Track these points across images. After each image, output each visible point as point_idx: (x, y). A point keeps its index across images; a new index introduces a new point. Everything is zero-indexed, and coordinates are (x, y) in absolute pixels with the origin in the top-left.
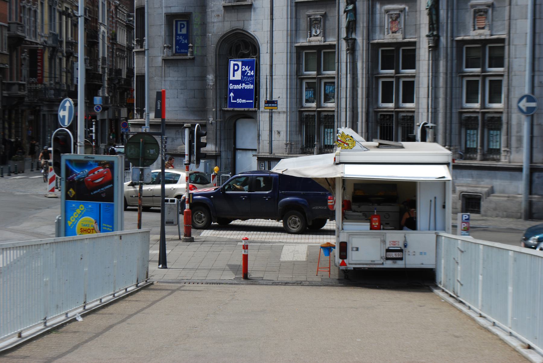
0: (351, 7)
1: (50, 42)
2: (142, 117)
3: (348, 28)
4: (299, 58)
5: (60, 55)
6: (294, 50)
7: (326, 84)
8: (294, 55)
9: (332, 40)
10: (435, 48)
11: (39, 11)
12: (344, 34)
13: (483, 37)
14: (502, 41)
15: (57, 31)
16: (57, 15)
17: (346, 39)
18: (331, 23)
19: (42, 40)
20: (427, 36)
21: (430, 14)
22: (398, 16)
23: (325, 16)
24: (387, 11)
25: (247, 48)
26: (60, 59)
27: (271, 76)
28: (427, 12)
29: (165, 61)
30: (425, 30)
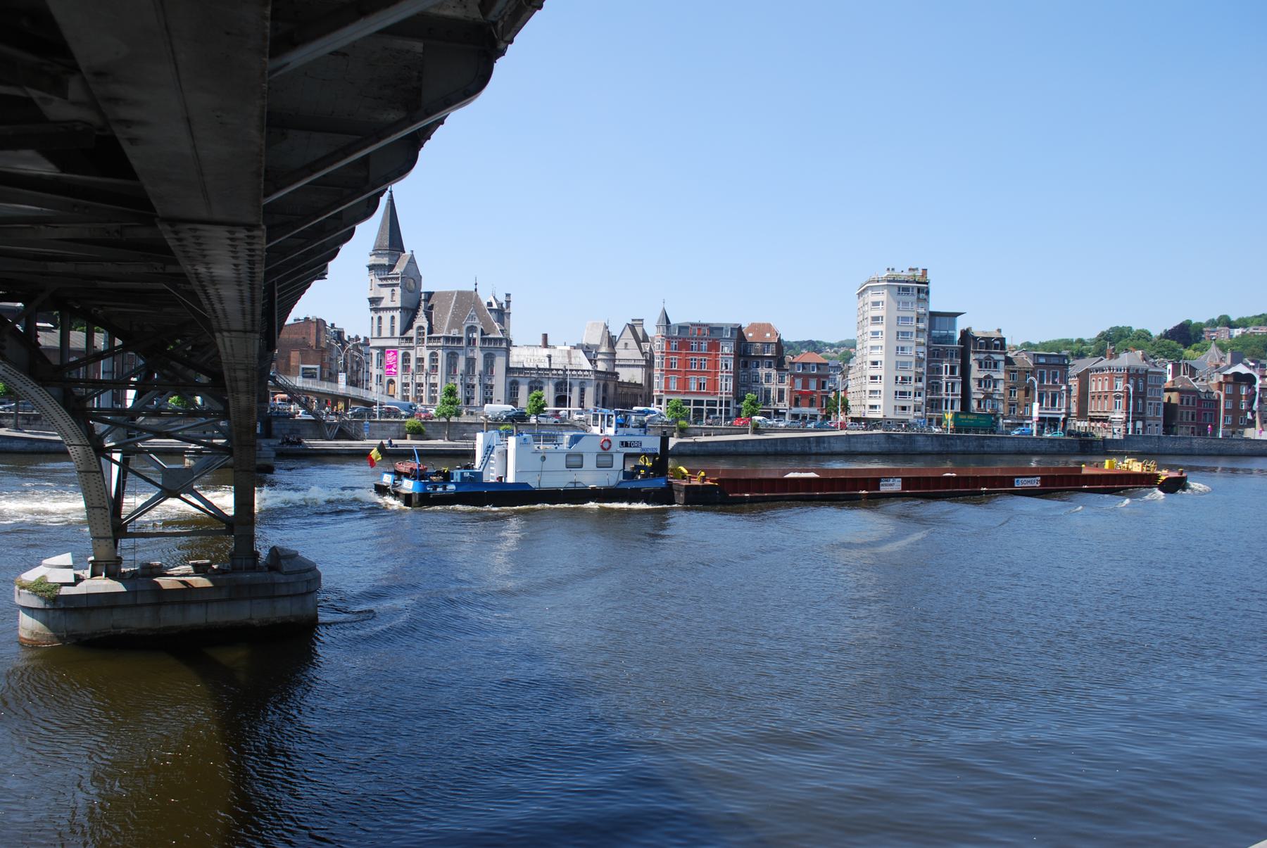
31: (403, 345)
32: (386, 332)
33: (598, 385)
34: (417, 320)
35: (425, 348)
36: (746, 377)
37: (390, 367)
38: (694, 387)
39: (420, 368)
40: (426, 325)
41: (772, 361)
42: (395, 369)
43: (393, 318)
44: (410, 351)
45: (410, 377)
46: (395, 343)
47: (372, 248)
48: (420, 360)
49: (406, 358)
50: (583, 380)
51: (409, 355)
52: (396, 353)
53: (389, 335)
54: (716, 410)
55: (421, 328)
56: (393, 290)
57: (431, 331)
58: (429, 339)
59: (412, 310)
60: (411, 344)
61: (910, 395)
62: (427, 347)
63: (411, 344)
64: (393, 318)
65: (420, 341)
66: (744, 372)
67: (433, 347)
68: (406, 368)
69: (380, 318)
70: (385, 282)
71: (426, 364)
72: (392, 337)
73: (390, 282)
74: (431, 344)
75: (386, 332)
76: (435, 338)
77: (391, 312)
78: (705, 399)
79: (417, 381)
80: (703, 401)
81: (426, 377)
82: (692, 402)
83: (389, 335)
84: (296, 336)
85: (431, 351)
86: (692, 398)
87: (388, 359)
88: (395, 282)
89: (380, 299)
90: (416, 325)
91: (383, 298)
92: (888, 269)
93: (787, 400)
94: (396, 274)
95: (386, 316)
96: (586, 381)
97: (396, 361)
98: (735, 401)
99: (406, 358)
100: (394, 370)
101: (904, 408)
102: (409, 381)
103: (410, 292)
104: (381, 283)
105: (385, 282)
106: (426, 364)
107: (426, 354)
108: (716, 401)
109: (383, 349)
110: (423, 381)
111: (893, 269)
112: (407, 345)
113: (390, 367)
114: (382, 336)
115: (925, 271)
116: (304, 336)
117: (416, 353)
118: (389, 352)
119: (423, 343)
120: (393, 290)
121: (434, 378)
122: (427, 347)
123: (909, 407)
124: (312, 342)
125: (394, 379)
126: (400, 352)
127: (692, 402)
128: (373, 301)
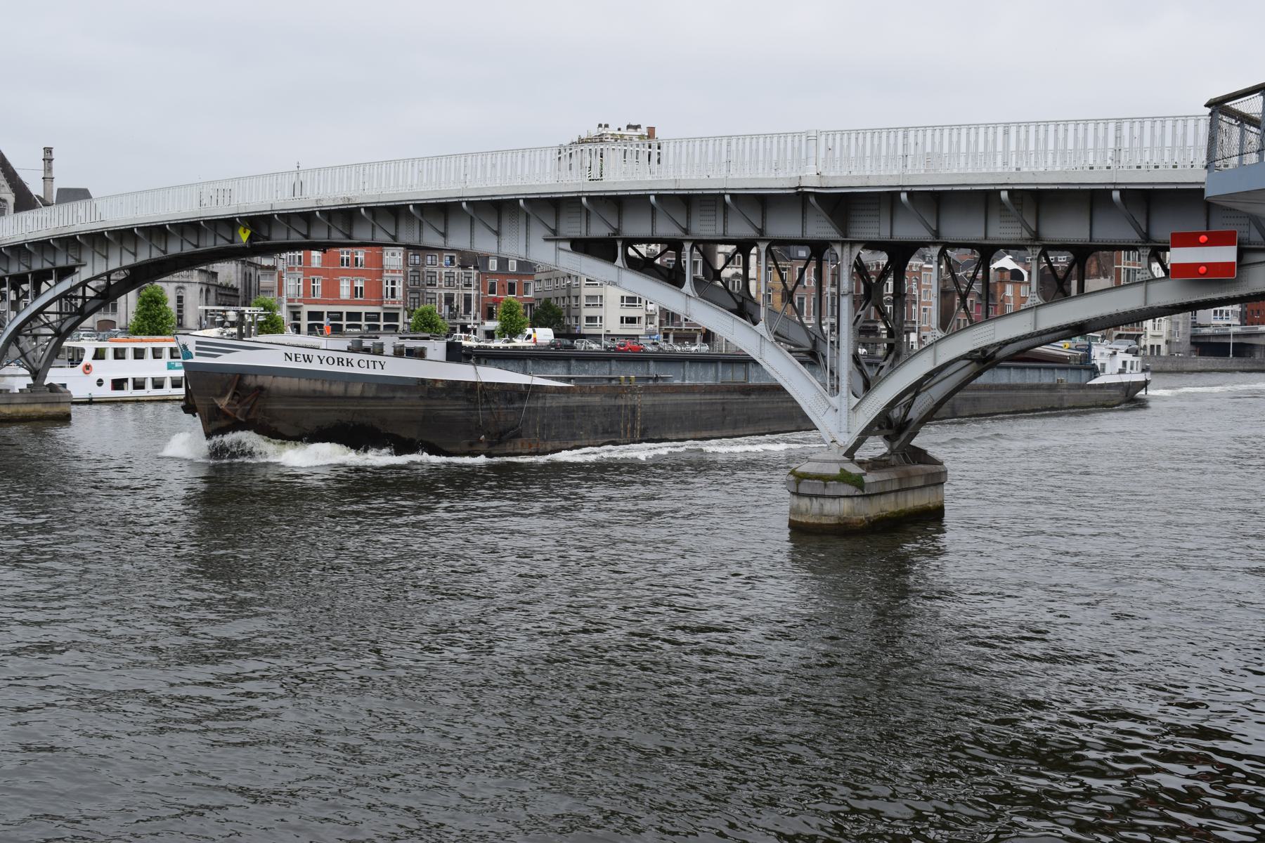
33: (201, 290)
36: (417, 278)
38: (345, 292)
41: (454, 254)
50: (181, 284)
54: (341, 325)
61: (640, 302)
66: (414, 271)
78: (363, 309)
80: (360, 313)
82: (344, 315)
86: (345, 309)
92: (600, 126)
93: (478, 310)
96: (185, 285)
98: (406, 313)
101: (631, 320)
108: (379, 314)
111: (607, 126)
115: (651, 131)
123: (639, 318)
127: (344, 315)
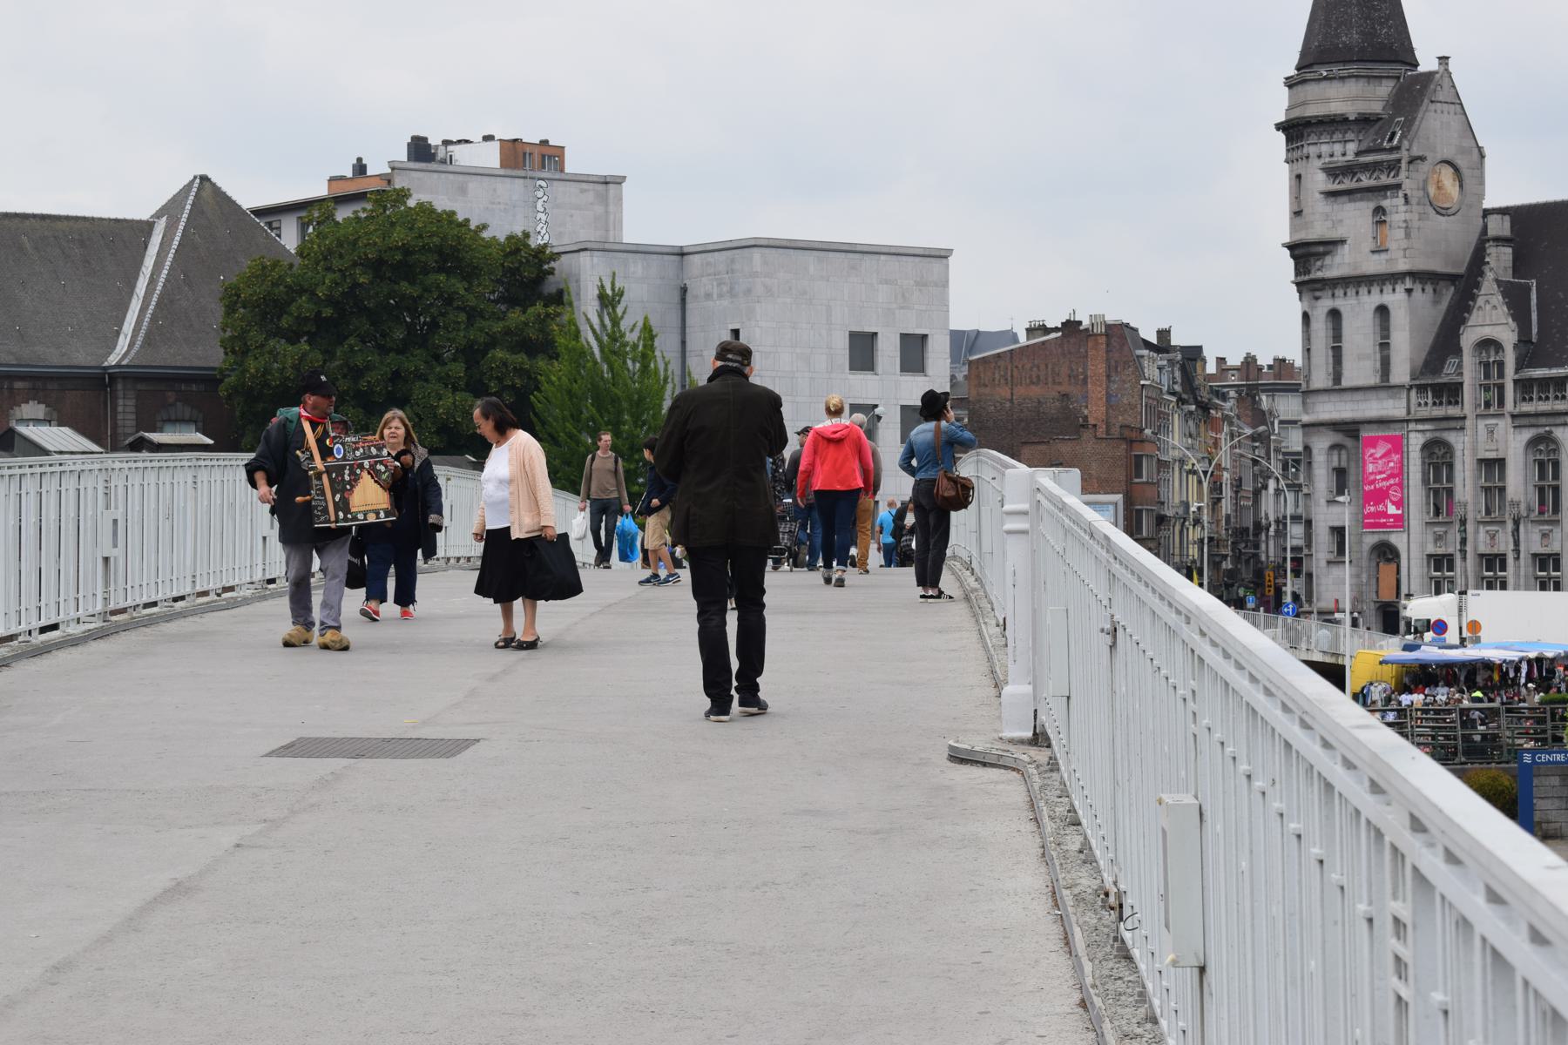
0: (1463, 528)
1: (1181, 511)
2: (1310, 606)
3: (1461, 543)
4: (1429, 563)
5: (1187, 523)
6: (1425, 557)
7: (1448, 582)
8: (1425, 561)
9: (1450, 550)
10: (1517, 558)
11: (1171, 479)
12: (1458, 547)
13: (1547, 552)
14: (1558, 555)
15: (1185, 499)
16: (1185, 474)
17: (1460, 551)
18: (1450, 537)
19: (1174, 511)
20: (1513, 550)
21: (1513, 535)
22: (1494, 535)
23: (1446, 532)
24: (1487, 532)
25: (1391, 553)
26: (1188, 529)
27: (1409, 575)
28: (1510, 534)
29: (1329, 562)
30: (1511, 546)
31: (1425, 412)
32: (1359, 370)
34: (1475, 318)
35: (1504, 424)
37: (1380, 496)
39: (1494, 491)
40: (1507, 335)
42: (1398, 504)
43: (1383, 311)
44: (1451, 437)
45: (1454, 536)
46: (1393, 407)
47: (1295, 59)
48: (1493, 466)
49: (1438, 457)
51: (1448, 448)
52: (1397, 445)
53: (1374, 380)
55: (1488, 344)
56: (1379, 210)
57: (1529, 353)
58: (1525, 388)
59: (1452, 278)
60: (1453, 411)
62: (1514, 416)
63: (1453, 411)
64: (1383, 311)
65: (1493, 398)
67: (1537, 415)
68: (1441, 499)
69: (1335, 315)
70: (1348, 184)
71: (1518, 483)
72: (1384, 386)
73: (1366, 181)
74: (1527, 408)
75: (1359, 370)
76: (1544, 383)
77: (1375, 289)
79: (1483, 549)
81: (1516, 531)
83: (1374, 380)
84: (1036, 391)
85: (1527, 435)
87: (1370, 468)
88: (1385, 180)
89: (1331, 245)
90: (1469, 338)
91: (1343, 242)
94: (1392, 150)
95: (1358, 311)
97: (1400, 473)
99: (1438, 457)
100: (1392, 510)
102: (1452, 547)
103: (1441, 212)
104: (1336, 187)
105: (1348, 184)
106: (1518, 483)
107: (1513, 444)
109: (1350, 429)
110: (1504, 544)
112: (1439, 412)
113: (1380, 496)
114: (1345, 383)
116: (1064, 389)
117: (1475, 442)
118: (1373, 442)
119: (1501, 403)
120: (1379, 210)
121: (1545, 535)
122: (1514, 416)
124: (1095, 411)
125: (1397, 540)
126: (1416, 441)
128: (1304, 253)
